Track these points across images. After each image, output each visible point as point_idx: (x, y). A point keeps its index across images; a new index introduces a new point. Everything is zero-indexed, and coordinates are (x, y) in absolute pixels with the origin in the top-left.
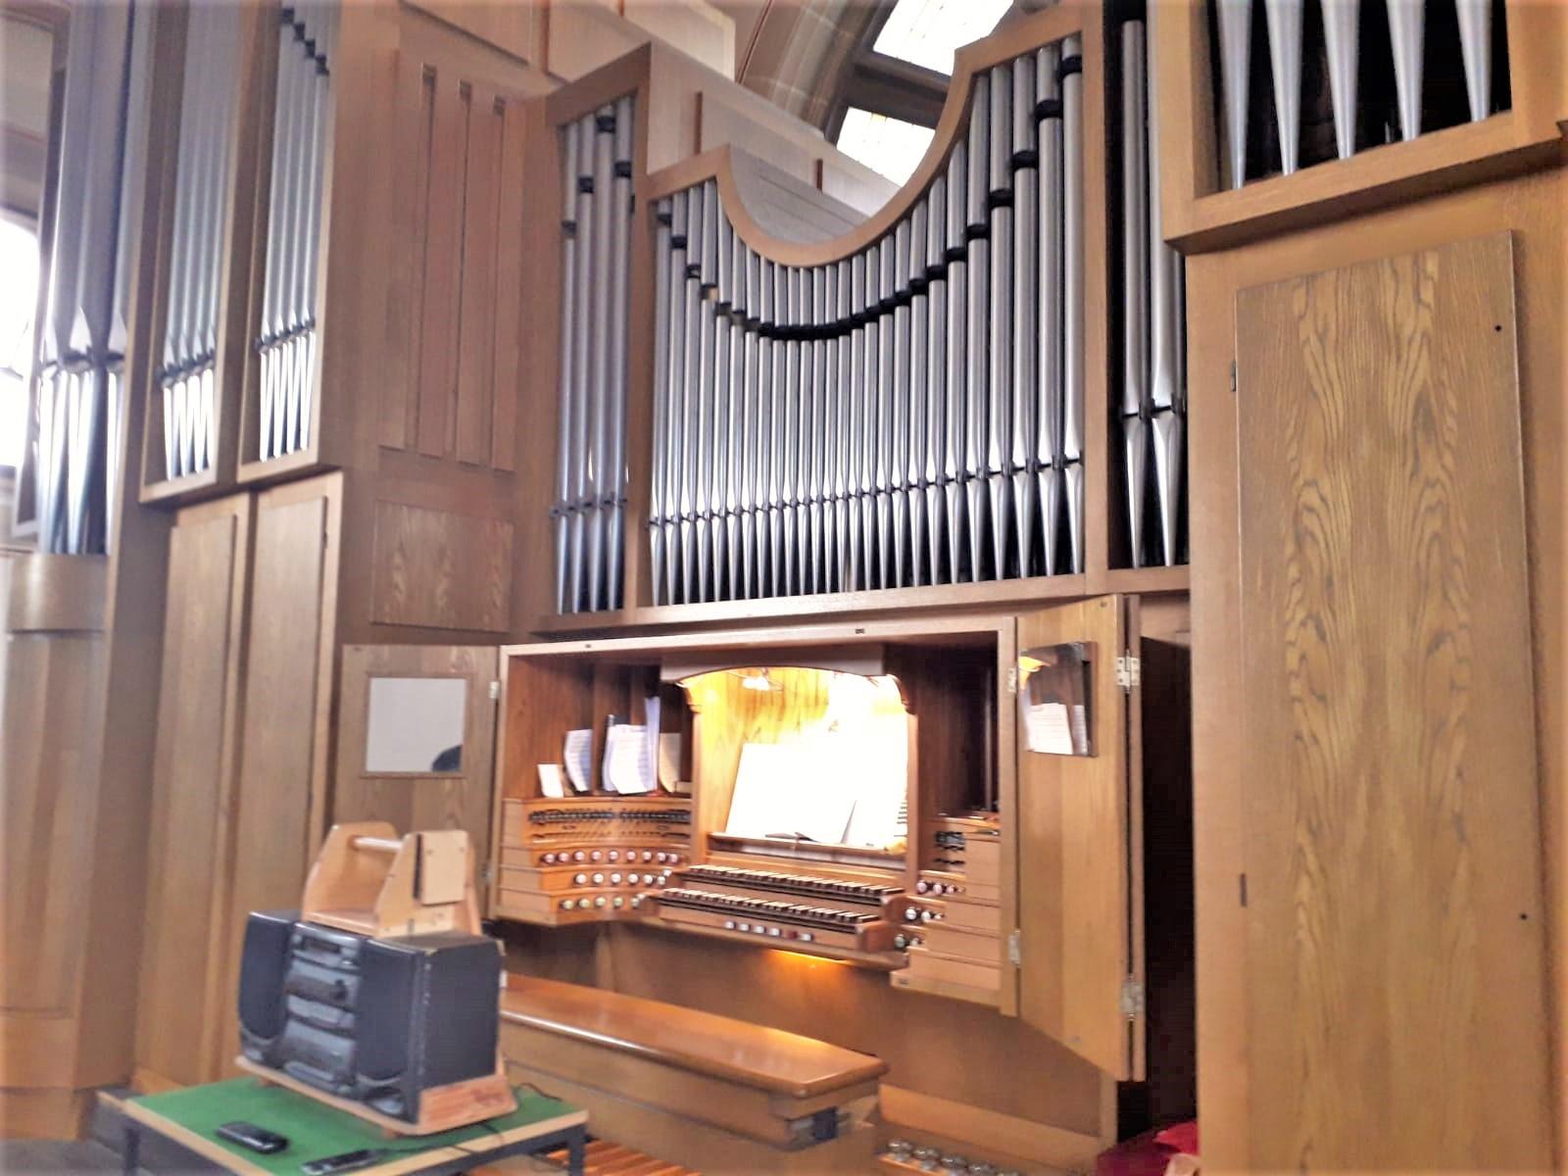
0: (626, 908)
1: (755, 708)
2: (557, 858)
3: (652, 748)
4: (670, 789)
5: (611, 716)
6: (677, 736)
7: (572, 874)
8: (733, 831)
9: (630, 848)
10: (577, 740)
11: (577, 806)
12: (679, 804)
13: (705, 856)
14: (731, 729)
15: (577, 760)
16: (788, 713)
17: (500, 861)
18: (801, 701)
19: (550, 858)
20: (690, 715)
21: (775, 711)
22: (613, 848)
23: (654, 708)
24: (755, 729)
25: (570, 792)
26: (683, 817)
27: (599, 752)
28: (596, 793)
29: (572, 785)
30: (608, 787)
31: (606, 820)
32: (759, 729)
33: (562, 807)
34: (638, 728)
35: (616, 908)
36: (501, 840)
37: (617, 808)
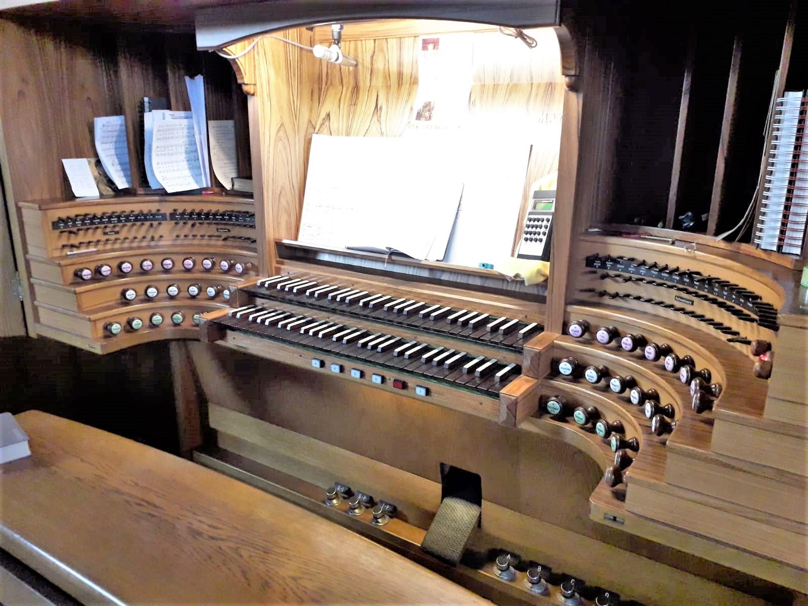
0: (186, 325)
1: (320, 89)
2: (98, 271)
3: (200, 138)
4: (228, 186)
5: (146, 99)
6: (230, 124)
7: (121, 289)
8: (305, 240)
9: (188, 255)
10: (108, 129)
11: (118, 209)
12: (240, 205)
13: (274, 265)
14: (295, 115)
15: (113, 152)
16: (363, 96)
17: (30, 275)
18: (379, 82)
19: (87, 274)
20: (243, 98)
21: (347, 92)
22: (166, 255)
23: (197, 88)
24: (323, 115)
25: (109, 191)
26: (248, 219)
27: (137, 146)
28: (141, 191)
29: (110, 183)
30: (154, 186)
31: (155, 223)
32: (328, 115)
33: (98, 211)
34: (182, 113)
35: (176, 325)
36: (26, 251)
37: (167, 208)
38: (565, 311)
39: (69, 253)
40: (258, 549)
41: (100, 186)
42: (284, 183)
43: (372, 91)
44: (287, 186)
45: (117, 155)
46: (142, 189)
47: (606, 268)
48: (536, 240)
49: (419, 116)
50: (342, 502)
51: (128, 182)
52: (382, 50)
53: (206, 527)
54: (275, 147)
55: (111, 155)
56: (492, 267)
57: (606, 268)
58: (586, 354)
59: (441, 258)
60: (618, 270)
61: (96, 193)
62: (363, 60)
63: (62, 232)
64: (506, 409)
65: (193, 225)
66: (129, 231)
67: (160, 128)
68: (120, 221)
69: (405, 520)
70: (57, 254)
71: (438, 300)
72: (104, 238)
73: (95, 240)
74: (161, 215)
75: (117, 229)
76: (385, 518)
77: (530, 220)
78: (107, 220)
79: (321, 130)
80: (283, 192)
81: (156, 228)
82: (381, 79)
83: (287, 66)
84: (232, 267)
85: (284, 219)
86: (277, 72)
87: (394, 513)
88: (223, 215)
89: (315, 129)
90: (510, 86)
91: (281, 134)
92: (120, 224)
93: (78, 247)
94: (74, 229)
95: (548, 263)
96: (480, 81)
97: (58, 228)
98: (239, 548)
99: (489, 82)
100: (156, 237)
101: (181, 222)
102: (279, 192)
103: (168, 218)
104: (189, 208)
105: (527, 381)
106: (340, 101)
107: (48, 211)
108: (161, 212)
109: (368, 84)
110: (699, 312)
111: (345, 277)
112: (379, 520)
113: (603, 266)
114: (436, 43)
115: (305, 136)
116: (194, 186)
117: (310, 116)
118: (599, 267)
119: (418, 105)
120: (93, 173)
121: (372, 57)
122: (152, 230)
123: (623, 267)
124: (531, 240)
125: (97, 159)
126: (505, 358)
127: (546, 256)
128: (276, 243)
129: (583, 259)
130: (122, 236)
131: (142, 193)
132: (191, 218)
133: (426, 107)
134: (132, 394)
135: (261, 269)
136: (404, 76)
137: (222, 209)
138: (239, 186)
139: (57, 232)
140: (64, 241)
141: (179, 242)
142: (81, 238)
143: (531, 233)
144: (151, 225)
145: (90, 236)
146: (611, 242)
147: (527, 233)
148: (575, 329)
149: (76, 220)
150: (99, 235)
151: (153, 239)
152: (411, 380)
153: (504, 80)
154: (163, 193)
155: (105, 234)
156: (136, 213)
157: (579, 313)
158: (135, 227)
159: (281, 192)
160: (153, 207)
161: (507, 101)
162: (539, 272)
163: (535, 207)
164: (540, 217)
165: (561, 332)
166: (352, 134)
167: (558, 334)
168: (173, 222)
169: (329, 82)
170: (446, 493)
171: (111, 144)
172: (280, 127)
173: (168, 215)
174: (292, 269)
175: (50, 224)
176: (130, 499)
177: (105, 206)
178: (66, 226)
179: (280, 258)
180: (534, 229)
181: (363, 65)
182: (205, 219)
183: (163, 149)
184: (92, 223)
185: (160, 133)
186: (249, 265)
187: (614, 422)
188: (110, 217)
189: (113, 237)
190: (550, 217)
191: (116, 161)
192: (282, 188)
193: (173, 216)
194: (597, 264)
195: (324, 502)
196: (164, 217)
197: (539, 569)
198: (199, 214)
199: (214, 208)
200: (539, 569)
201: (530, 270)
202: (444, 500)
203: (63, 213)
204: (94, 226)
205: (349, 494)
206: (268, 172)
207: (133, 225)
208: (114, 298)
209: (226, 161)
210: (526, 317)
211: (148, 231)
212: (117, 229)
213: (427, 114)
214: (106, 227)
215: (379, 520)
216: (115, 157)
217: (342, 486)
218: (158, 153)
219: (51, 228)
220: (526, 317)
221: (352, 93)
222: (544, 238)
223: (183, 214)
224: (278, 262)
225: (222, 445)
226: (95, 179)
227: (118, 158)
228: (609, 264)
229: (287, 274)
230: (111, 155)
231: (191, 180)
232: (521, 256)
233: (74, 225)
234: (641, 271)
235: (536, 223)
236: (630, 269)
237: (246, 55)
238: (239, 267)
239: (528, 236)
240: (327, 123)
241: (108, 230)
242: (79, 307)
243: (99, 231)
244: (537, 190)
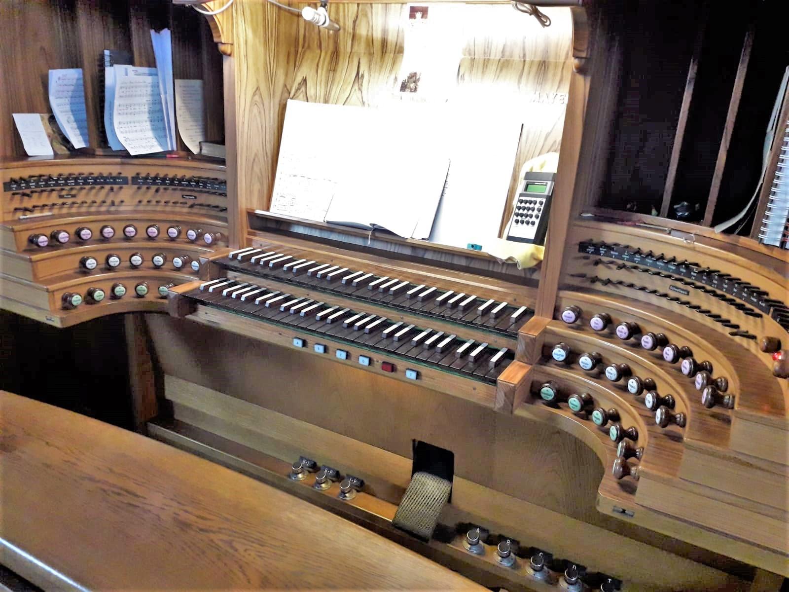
0: (150, 297)
1: (296, 52)
2: (54, 237)
3: (166, 97)
4: (195, 150)
5: (107, 52)
6: (197, 83)
7: (79, 258)
8: (278, 210)
9: (152, 223)
10: (63, 81)
11: (76, 170)
12: (209, 171)
13: (246, 236)
14: (270, 79)
15: (68, 107)
16: (343, 64)
18: (361, 48)
19: (43, 240)
20: (217, 58)
21: (325, 58)
22: (130, 222)
23: (163, 42)
24: (299, 79)
25: (63, 150)
26: (219, 187)
27: (96, 104)
28: (99, 152)
29: (66, 141)
31: (116, 187)
33: (54, 172)
34: (145, 70)
35: (139, 296)
37: (129, 172)
38: (557, 296)
39: (22, 217)
40: (253, 542)
41: (54, 144)
42: (258, 151)
43: (352, 58)
44: (261, 152)
45: (72, 111)
46: (100, 150)
47: (600, 254)
48: (528, 223)
49: (404, 87)
50: (308, 476)
51: (85, 141)
52: (366, 15)
53: (193, 518)
54: (251, 111)
55: (66, 112)
56: (481, 247)
57: (600, 254)
58: (580, 341)
59: (427, 236)
60: (612, 257)
61: (51, 153)
62: (344, 24)
63: (14, 194)
64: (504, 395)
65: (157, 191)
66: (87, 194)
67: (123, 85)
68: (77, 184)
69: (374, 495)
70: (9, 217)
71: (422, 279)
72: (60, 201)
74: (122, 178)
75: (73, 192)
76: (353, 492)
77: (521, 202)
79: (297, 95)
80: (256, 159)
81: (117, 193)
82: (363, 45)
83: (264, 27)
84: (200, 236)
85: (256, 187)
86: (255, 31)
87: (361, 487)
88: (189, 181)
89: (290, 93)
90: (502, 61)
91: (257, 98)
92: (78, 187)
93: (31, 211)
94: (28, 191)
95: (543, 248)
96: (470, 54)
97: (11, 189)
98: (233, 541)
99: (479, 56)
100: (117, 202)
101: (144, 187)
102: (252, 160)
103: (130, 182)
104: (153, 172)
105: (521, 367)
106: (318, 66)
108: (122, 175)
109: (349, 50)
110: (695, 302)
111: (323, 251)
112: (347, 495)
113: (597, 252)
114: (424, 11)
115: (280, 101)
116: (158, 149)
117: (285, 80)
118: (592, 253)
119: (403, 76)
120: (46, 130)
121: (355, 22)
122: (112, 194)
123: (617, 254)
124: (522, 222)
125: (50, 114)
126: (496, 342)
127: (539, 239)
129: (575, 244)
130: (79, 200)
131: (101, 153)
133: (411, 78)
134: (93, 368)
135: (231, 239)
136: (388, 45)
137: (188, 174)
138: (208, 151)
140: (16, 203)
141: (141, 208)
142: (35, 200)
143: (522, 215)
144: (112, 189)
145: (44, 199)
146: (604, 228)
147: (517, 215)
148: (568, 315)
149: (30, 182)
150: (54, 198)
151: (113, 203)
152: (400, 363)
153: (495, 55)
154: (125, 154)
155: (61, 197)
156: (95, 175)
157: (571, 298)
159: (254, 160)
160: (114, 170)
161: (498, 77)
162: (533, 257)
163: (526, 189)
164: (533, 199)
165: (552, 317)
166: (331, 101)
167: (549, 320)
168: (136, 186)
169: (306, 45)
170: (417, 468)
171: (67, 100)
172: (256, 91)
173: (130, 178)
174: (264, 240)
176: (106, 487)
177: (55, 167)
178: (19, 187)
179: (252, 228)
180: (525, 212)
181: (344, 29)
182: (161, 184)
183: (125, 108)
184: (47, 185)
185: (123, 90)
186: (218, 235)
187: (609, 410)
188: (66, 179)
189: (70, 201)
190: (544, 200)
191: (72, 118)
192: (256, 155)
193: (135, 180)
194: (591, 249)
195: (289, 476)
196: (125, 181)
197: (508, 542)
198: (163, 180)
199: (180, 173)
200: (508, 542)
201: (522, 253)
202: (414, 476)
203: (16, 174)
204: (49, 188)
205: (314, 468)
206: (242, 137)
207: (92, 188)
209: (191, 123)
210: (515, 300)
211: (108, 194)
212: (73, 192)
213: (412, 85)
215: (347, 495)
216: (71, 113)
217: (307, 460)
218: (119, 112)
220: (515, 300)
221: (332, 59)
222: (537, 221)
223: (146, 178)
224: (249, 233)
225: (177, 416)
226: (49, 136)
227: (74, 115)
228: (602, 250)
229: (259, 246)
230: (66, 112)
231: (154, 142)
232: (510, 238)
233: (28, 187)
234: (635, 259)
235: (528, 205)
236: (624, 256)
237: (225, 13)
238: (208, 237)
239: (519, 218)
240: (303, 89)
241: (64, 193)
242: (35, 275)
243: (55, 194)
244: (528, 170)
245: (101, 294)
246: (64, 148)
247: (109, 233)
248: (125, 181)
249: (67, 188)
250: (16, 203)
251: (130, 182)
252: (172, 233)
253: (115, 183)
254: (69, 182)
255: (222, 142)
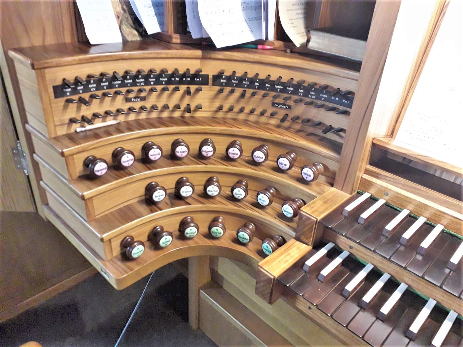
11: (145, 66)
17: (32, 151)
19: (100, 168)
25: (134, 36)
29: (137, 24)
31: (193, 88)
33: (120, 68)
36: (25, 121)
37: (211, 68)
39: (79, 130)
41: (124, 27)
46: (178, 36)
61: (119, 40)
63: (69, 101)
65: (243, 96)
68: (147, 83)
70: (62, 131)
73: (113, 109)
75: (143, 94)
78: (131, 81)
92: (148, 88)
93: (90, 122)
94: (86, 96)
97: (63, 94)
101: (228, 89)
103: (210, 82)
104: (240, 69)
107: (46, 70)
122: (187, 98)
128: (373, 144)
132: (240, 84)
135: (339, 179)
137: (286, 75)
139: (61, 101)
140: (72, 112)
142: (96, 107)
145: (108, 105)
149: (88, 82)
150: (120, 103)
154: (206, 45)
155: (128, 100)
158: (167, 93)
160: (193, 66)
168: (217, 88)
173: (210, 77)
175: (51, 90)
178: (75, 91)
184: (110, 86)
189: (137, 105)
193: (217, 78)
196: (205, 81)
198: (252, 81)
199: (275, 74)
203: (70, 73)
207: (164, 90)
208: (139, 195)
211: (183, 97)
212: (143, 94)
214: (128, 92)
219: (52, 95)
223: (229, 79)
224: (367, 172)
233: (86, 89)
241: (131, 96)
242: (88, 214)
245: (167, 240)
246: (136, 32)
247: (183, 152)
248: (205, 81)
249: (135, 89)
250: (72, 112)
251: (210, 82)
252: (258, 157)
253: (192, 82)
254: (137, 81)
255: (361, 32)
